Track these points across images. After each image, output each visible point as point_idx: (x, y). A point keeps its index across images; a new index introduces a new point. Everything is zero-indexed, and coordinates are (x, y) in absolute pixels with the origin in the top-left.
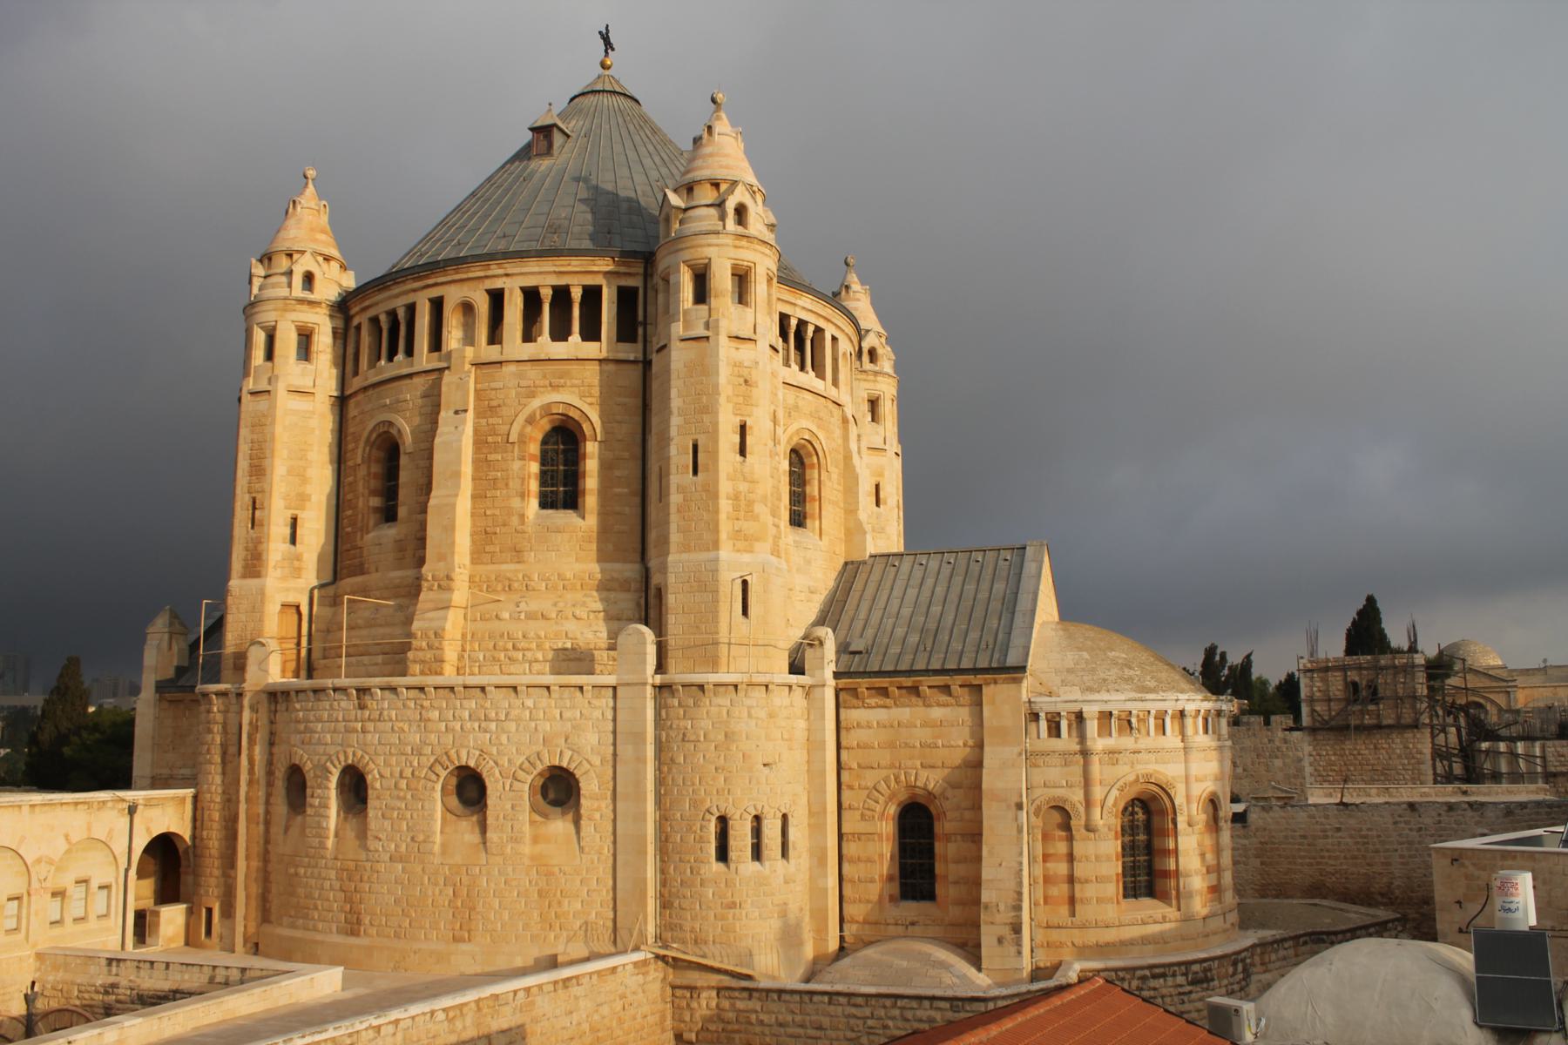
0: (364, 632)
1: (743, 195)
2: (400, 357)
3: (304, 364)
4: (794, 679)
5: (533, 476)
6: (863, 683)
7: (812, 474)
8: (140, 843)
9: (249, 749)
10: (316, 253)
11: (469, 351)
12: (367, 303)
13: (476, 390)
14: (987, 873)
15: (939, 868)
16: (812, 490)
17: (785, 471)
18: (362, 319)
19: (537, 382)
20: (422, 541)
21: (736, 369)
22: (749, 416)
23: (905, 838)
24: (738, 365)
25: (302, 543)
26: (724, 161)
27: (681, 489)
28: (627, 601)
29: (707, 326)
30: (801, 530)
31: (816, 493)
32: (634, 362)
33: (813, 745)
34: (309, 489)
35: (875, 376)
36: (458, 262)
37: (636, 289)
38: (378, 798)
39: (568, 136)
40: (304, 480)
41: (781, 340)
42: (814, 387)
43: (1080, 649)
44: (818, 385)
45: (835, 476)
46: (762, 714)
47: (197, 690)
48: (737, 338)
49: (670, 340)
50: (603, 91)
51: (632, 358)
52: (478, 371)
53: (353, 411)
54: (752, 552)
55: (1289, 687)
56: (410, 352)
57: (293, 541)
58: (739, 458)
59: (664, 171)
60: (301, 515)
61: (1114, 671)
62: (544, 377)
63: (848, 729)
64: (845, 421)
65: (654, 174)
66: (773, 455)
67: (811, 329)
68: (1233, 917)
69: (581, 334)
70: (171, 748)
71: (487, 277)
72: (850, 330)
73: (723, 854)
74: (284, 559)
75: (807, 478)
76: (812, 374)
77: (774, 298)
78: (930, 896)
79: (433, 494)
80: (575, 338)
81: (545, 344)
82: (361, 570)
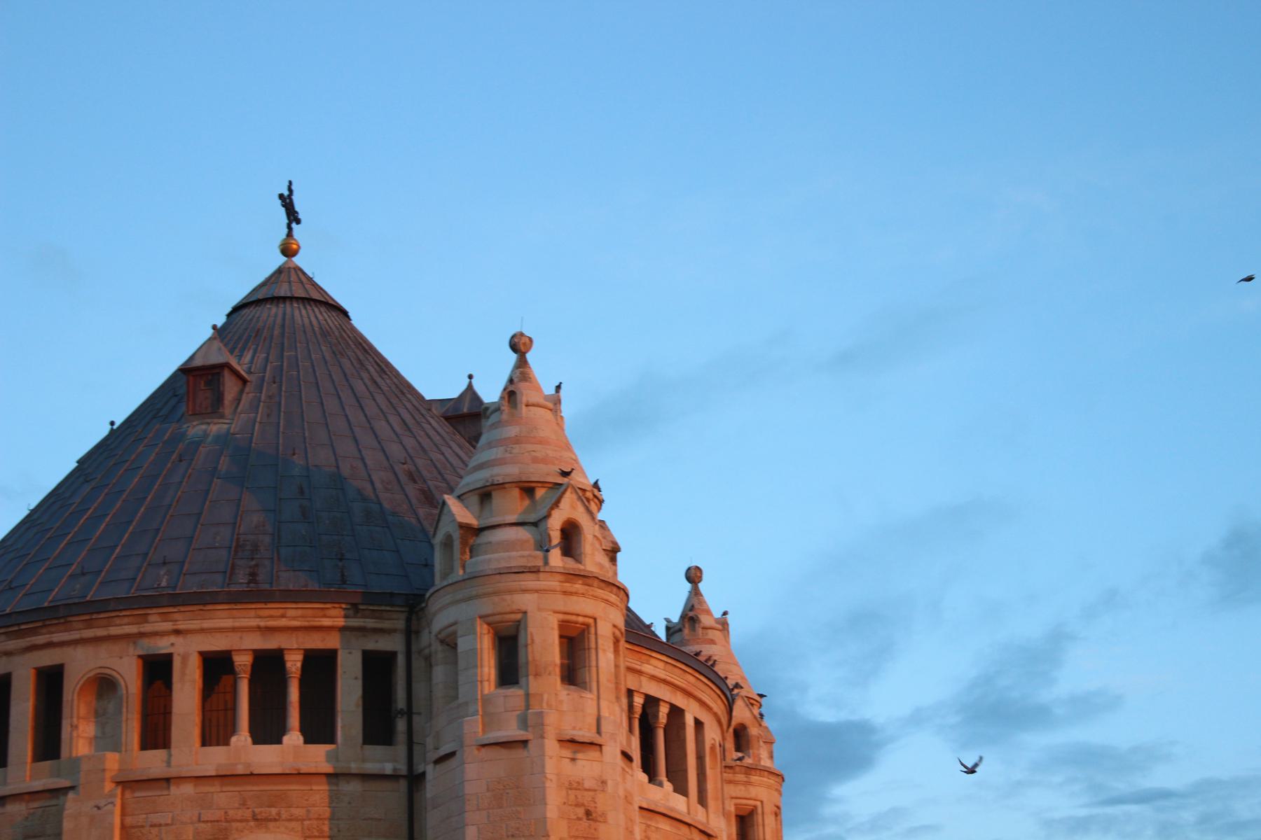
1: (573, 507)
11: (112, 761)
13: (123, 827)
19: (231, 813)
24: (575, 786)
26: (540, 451)
29: (524, 723)
32: (393, 777)
35: (747, 774)
37: (393, 655)
39: (244, 381)
42: (672, 809)
44: (678, 804)
48: (572, 741)
49: (462, 746)
50: (292, 299)
51: (388, 768)
52: (128, 795)
59: (409, 442)
62: (244, 804)
65: (395, 450)
67: (664, 710)
69: (303, 731)
72: (718, 707)
76: (668, 786)
77: (622, 669)
80: (293, 738)
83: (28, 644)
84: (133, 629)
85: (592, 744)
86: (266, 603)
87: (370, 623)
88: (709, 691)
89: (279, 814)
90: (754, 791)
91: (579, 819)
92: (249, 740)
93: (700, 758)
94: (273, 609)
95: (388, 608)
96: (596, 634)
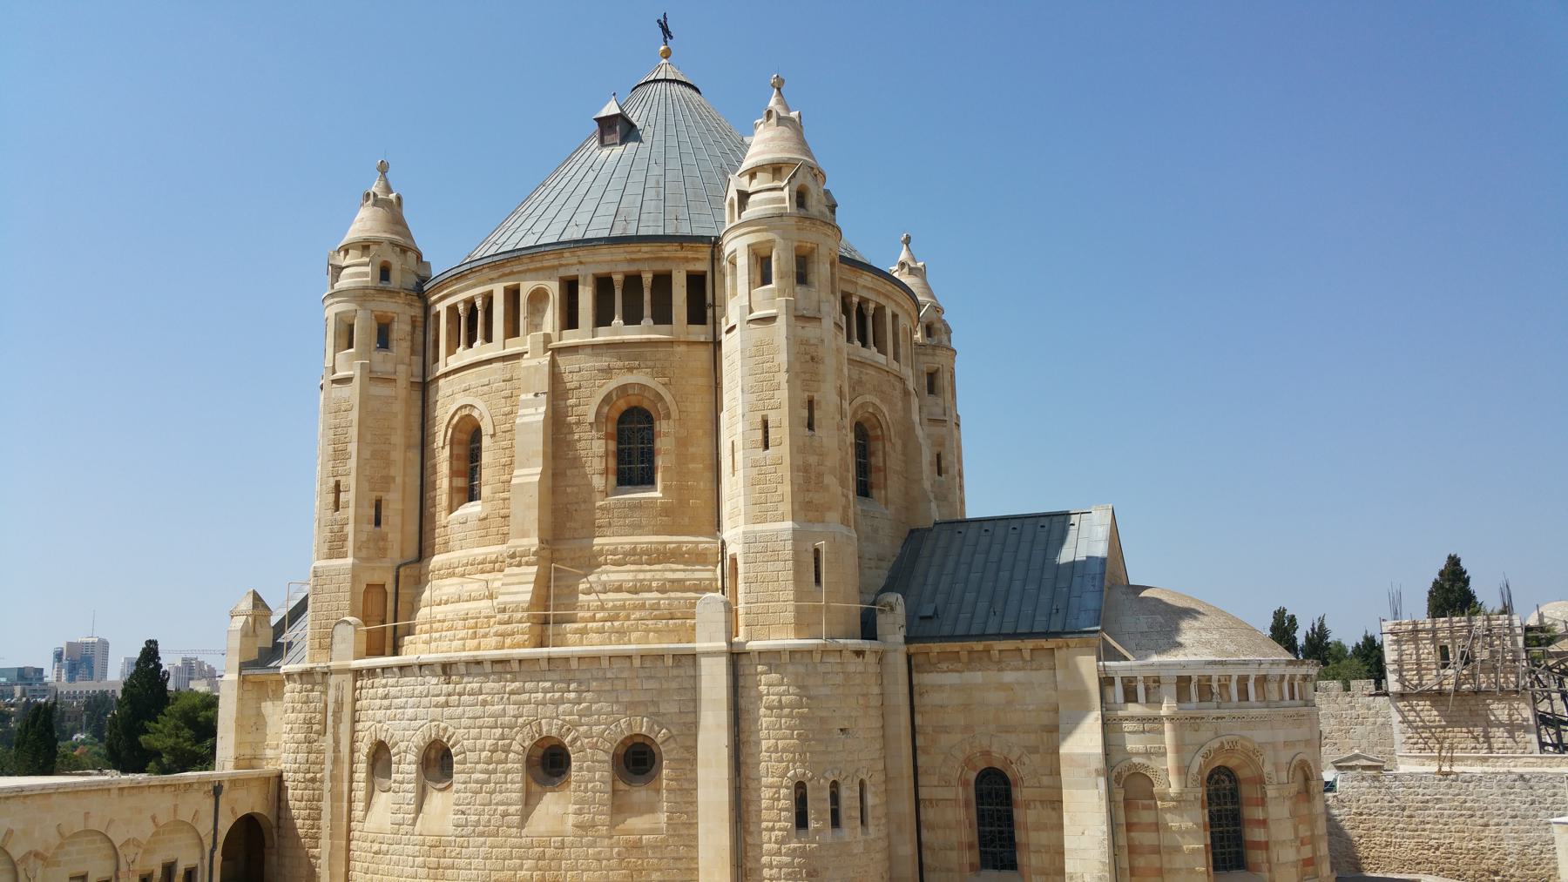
0: (450, 607)
1: (805, 177)
2: (477, 344)
3: (383, 353)
4: (866, 645)
5: (610, 453)
6: (936, 647)
8: (225, 825)
9: (334, 727)
10: (393, 244)
12: (445, 292)
16: (876, 461)
17: (851, 444)
18: (442, 307)
21: (803, 348)
22: (817, 392)
23: (983, 804)
24: (805, 342)
25: (387, 524)
30: (867, 500)
31: (881, 464)
33: (884, 711)
34: (392, 472)
37: (706, 272)
38: (463, 772)
40: (388, 463)
41: (844, 317)
43: (1153, 613)
44: (881, 358)
45: (899, 447)
46: (839, 679)
47: (281, 671)
51: (702, 339)
54: (823, 522)
56: (488, 338)
57: (378, 523)
58: (811, 433)
60: (385, 496)
63: (921, 695)
64: (906, 393)
66: (840, 428)
67: (872, 306)
69: (653, 317)
70: (254, 728)
71: (561, 265)
72: (908, 305)
73: (801, 821)
74: (369, 540)
75: (872, 449)
76: (874, 349)
79: (516, 473)
80: (647, 321)
81: (619, 331)
83: (500, 273)
84: (556, 262)
85: (815, 318)
86: (629, 244)
87: (690, 255)
88: (898, 294)
89: (639, 365)
90: (937, 359)
91: (806, 362)
92: (621, 321)
93: (895, 335)
94: (632, 248)
95: (701, 245)
96: (818, 253)
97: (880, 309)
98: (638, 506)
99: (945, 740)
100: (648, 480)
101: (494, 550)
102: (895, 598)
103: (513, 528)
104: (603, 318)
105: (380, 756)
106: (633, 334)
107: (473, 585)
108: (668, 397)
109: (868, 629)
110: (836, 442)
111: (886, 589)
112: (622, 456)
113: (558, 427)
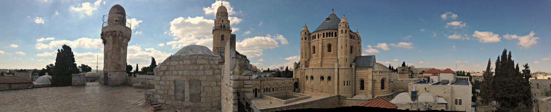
6: (358, 68)
7: (353, 49)
14: (368, 87)
15: (365, 87)
16: (353, 50)
18: (311, 36)
20: (318, 55)
24: (346, 39)
27: (341, 50)
28: (336, 60)
36: (320, 30)
53: (311, 44)
55: (397, 69)
56: (316, 39)
57: (306, 55)
61: (381, 68)
66: (349, 47)
68: (391, 91)
78: (364, 89)
82: (312, 58)
97: (354, 36)
98: (330, 54)
99: (358, 77)
100: (331, 52)
101: (317, 58)
102: (354, 63)
103: (319, 56)
104: (327, 36)
105: (307, 77)
106: (330, 38)
107: (315, 61)
108: (332, 43)
109: (351, 66)
110: (348, 48)
111: (353, 62)
112: (329, 49)
113: (322, 46)
